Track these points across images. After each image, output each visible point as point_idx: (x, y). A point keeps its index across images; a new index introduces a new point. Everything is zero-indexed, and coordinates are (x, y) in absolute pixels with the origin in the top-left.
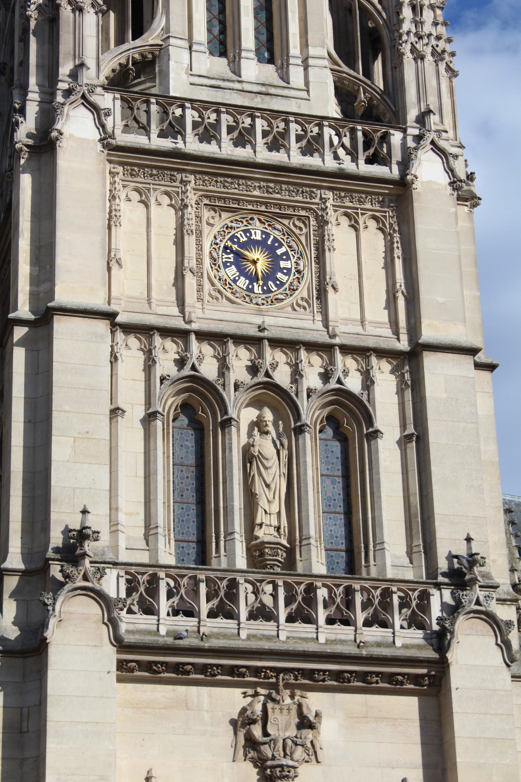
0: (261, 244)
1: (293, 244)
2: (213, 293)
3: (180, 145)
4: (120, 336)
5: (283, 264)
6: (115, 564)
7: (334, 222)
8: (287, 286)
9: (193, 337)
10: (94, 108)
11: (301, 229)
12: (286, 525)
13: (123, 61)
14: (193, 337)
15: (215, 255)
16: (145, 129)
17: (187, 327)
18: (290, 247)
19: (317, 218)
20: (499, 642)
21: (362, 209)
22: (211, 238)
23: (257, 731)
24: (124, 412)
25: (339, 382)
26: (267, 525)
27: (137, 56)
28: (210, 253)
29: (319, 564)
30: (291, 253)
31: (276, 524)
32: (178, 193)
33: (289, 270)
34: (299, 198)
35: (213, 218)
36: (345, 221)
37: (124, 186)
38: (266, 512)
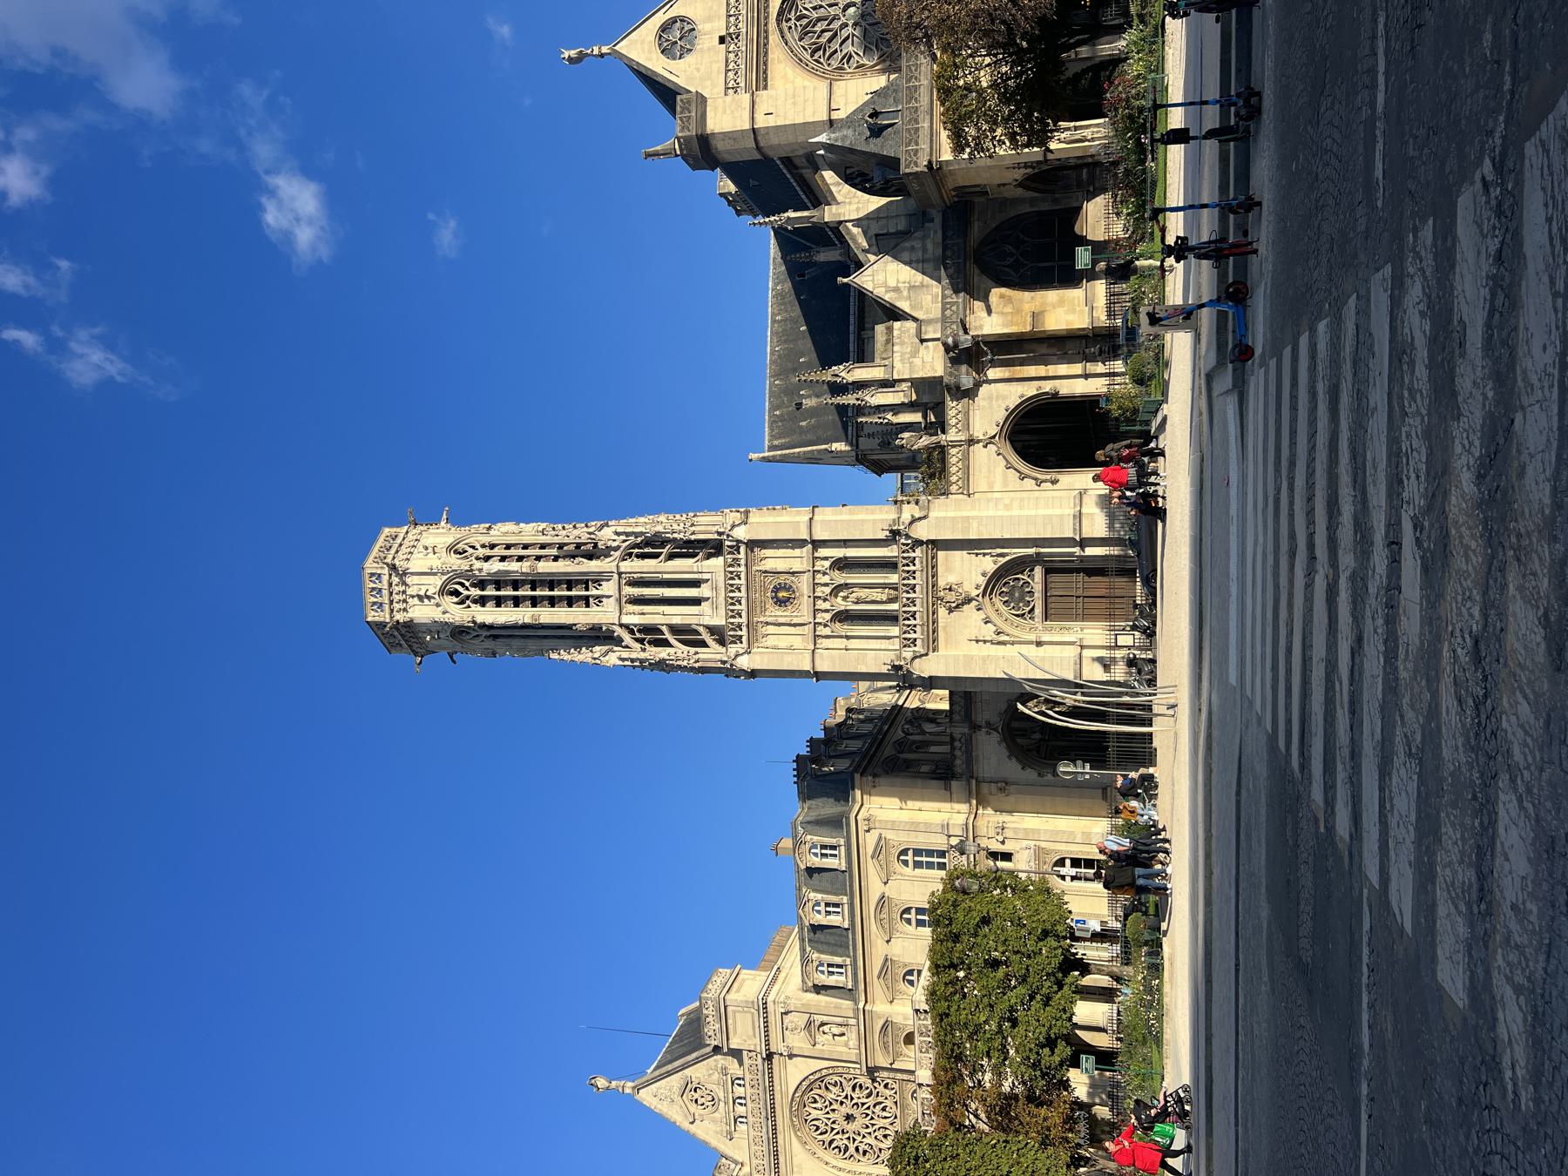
0: (776, 593)
4: (818, 646)
10: (737, 656)
16: (741, 637)
23: (954, 605)
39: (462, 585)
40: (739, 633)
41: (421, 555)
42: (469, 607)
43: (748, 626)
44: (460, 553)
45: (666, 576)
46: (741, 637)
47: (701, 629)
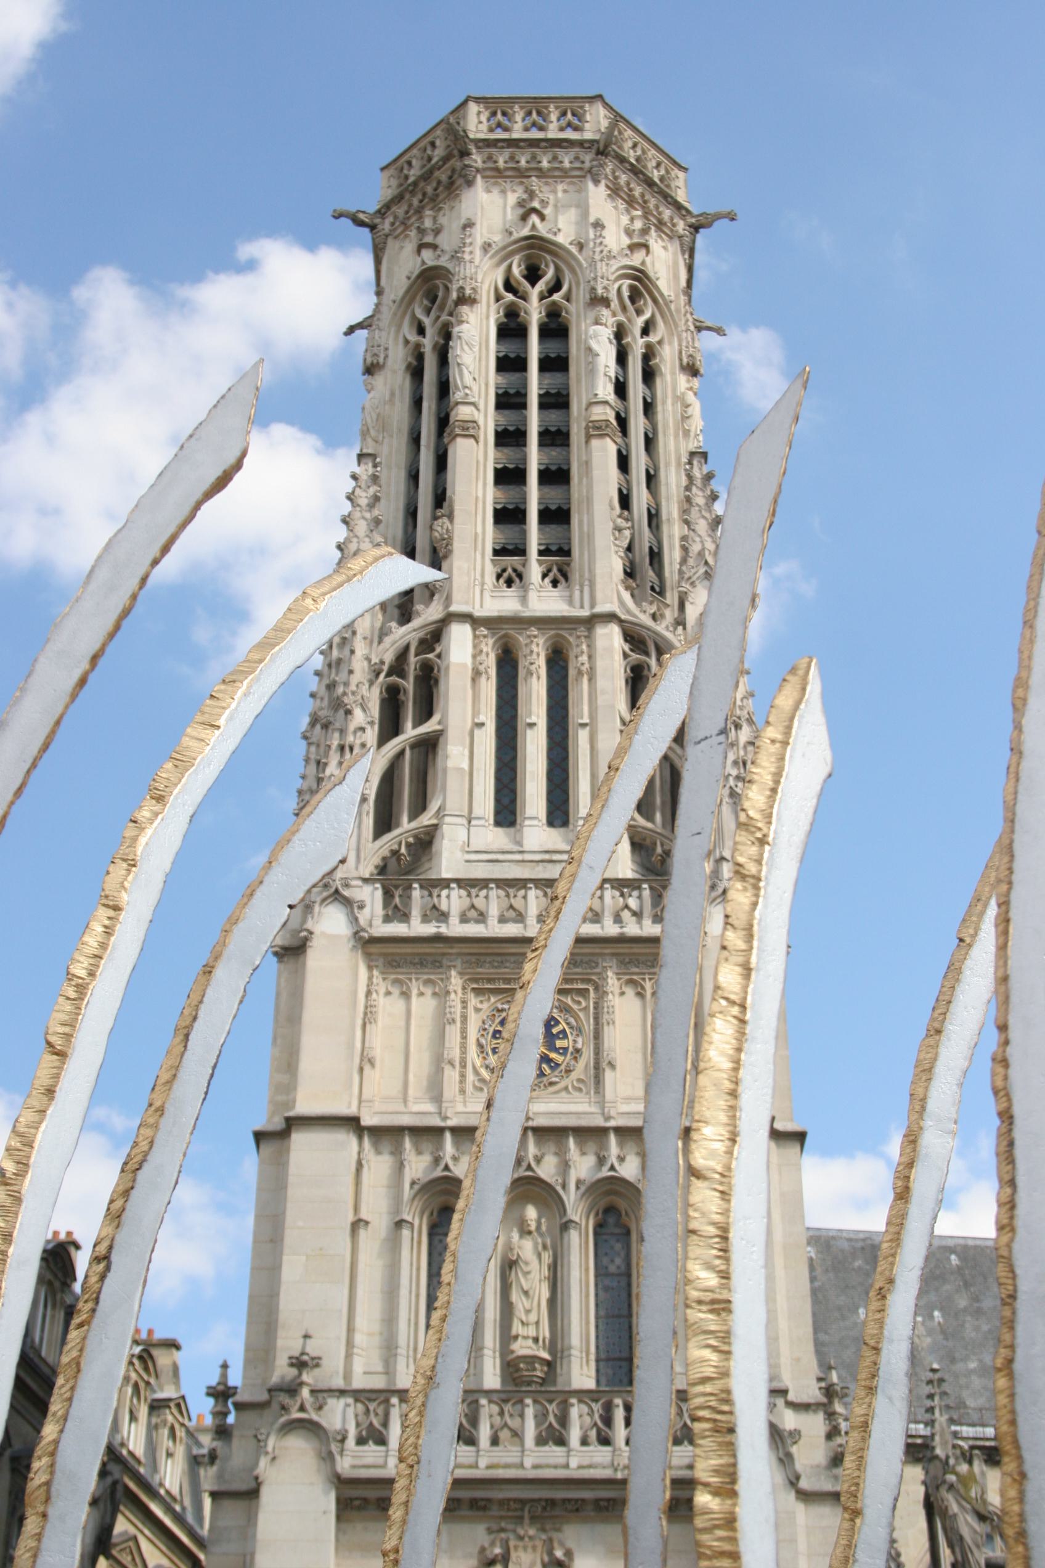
1: (572, 1020)
2: (477, 1084)
3: (444, 930)
5: (559, 1043)
6: (342, 1393)
7: (617, 991)
8: (563, 1067)
9: (448, 1136)
10: (347, 902)
11: (579, 1003)
12: (547, 1335)
13: (396, 847)
14: (448, 1136)
15: (483, 1041)
16: (405, 917)
17: (442, 1124)
18: (568, 1024)
19: (596, 989)
20: (781, 1455)
21: (649, 974)
22: (480, 1023)
24: (367, 1223)
25: (612, 1168)
26: (525, 1338)
27: (411, 840)
28: (478, 1040)
29: (584, 1378)
30: (568, 1031)
31: (534, 1334)
32: (442, 980)
33: (566, 1049)
34: (579, 970)
35: (481, 1002)
36: (630, 992)
37: (384, 979)
38: (523, 1323)
39: (556, 287)
40: (416, 913)
41: (625, 220)
42: (498, 298)
43: (438, 939)
44: (632, 299)
45: (583, 736)
46: (405, 917)
47: (426, 819)
